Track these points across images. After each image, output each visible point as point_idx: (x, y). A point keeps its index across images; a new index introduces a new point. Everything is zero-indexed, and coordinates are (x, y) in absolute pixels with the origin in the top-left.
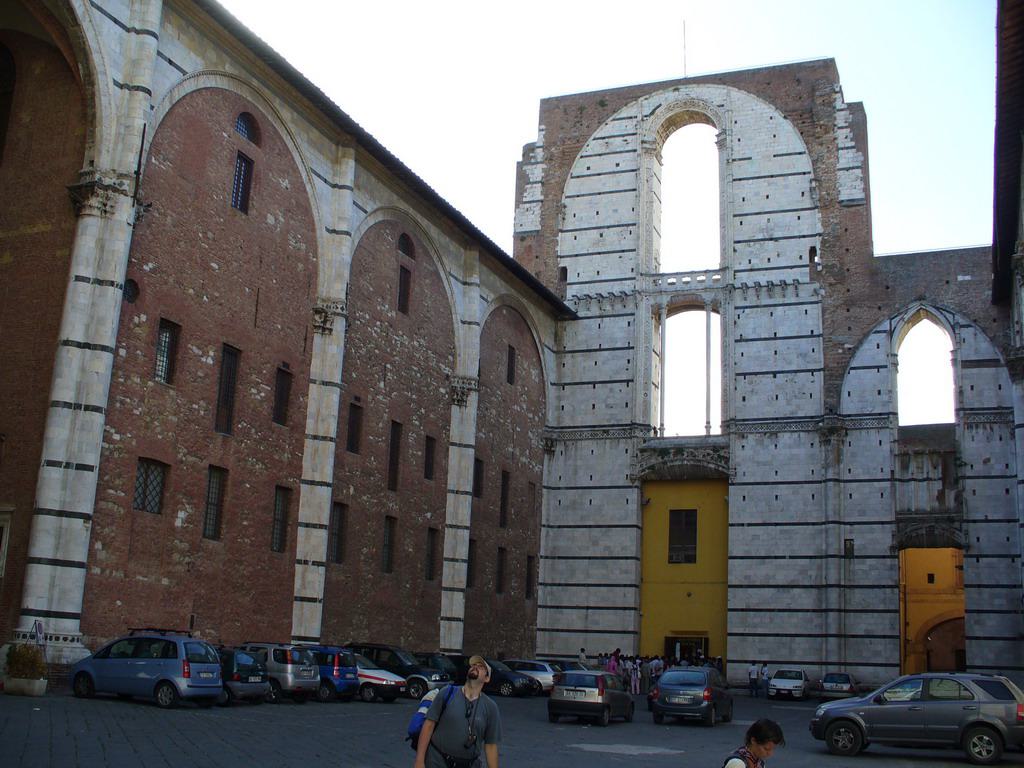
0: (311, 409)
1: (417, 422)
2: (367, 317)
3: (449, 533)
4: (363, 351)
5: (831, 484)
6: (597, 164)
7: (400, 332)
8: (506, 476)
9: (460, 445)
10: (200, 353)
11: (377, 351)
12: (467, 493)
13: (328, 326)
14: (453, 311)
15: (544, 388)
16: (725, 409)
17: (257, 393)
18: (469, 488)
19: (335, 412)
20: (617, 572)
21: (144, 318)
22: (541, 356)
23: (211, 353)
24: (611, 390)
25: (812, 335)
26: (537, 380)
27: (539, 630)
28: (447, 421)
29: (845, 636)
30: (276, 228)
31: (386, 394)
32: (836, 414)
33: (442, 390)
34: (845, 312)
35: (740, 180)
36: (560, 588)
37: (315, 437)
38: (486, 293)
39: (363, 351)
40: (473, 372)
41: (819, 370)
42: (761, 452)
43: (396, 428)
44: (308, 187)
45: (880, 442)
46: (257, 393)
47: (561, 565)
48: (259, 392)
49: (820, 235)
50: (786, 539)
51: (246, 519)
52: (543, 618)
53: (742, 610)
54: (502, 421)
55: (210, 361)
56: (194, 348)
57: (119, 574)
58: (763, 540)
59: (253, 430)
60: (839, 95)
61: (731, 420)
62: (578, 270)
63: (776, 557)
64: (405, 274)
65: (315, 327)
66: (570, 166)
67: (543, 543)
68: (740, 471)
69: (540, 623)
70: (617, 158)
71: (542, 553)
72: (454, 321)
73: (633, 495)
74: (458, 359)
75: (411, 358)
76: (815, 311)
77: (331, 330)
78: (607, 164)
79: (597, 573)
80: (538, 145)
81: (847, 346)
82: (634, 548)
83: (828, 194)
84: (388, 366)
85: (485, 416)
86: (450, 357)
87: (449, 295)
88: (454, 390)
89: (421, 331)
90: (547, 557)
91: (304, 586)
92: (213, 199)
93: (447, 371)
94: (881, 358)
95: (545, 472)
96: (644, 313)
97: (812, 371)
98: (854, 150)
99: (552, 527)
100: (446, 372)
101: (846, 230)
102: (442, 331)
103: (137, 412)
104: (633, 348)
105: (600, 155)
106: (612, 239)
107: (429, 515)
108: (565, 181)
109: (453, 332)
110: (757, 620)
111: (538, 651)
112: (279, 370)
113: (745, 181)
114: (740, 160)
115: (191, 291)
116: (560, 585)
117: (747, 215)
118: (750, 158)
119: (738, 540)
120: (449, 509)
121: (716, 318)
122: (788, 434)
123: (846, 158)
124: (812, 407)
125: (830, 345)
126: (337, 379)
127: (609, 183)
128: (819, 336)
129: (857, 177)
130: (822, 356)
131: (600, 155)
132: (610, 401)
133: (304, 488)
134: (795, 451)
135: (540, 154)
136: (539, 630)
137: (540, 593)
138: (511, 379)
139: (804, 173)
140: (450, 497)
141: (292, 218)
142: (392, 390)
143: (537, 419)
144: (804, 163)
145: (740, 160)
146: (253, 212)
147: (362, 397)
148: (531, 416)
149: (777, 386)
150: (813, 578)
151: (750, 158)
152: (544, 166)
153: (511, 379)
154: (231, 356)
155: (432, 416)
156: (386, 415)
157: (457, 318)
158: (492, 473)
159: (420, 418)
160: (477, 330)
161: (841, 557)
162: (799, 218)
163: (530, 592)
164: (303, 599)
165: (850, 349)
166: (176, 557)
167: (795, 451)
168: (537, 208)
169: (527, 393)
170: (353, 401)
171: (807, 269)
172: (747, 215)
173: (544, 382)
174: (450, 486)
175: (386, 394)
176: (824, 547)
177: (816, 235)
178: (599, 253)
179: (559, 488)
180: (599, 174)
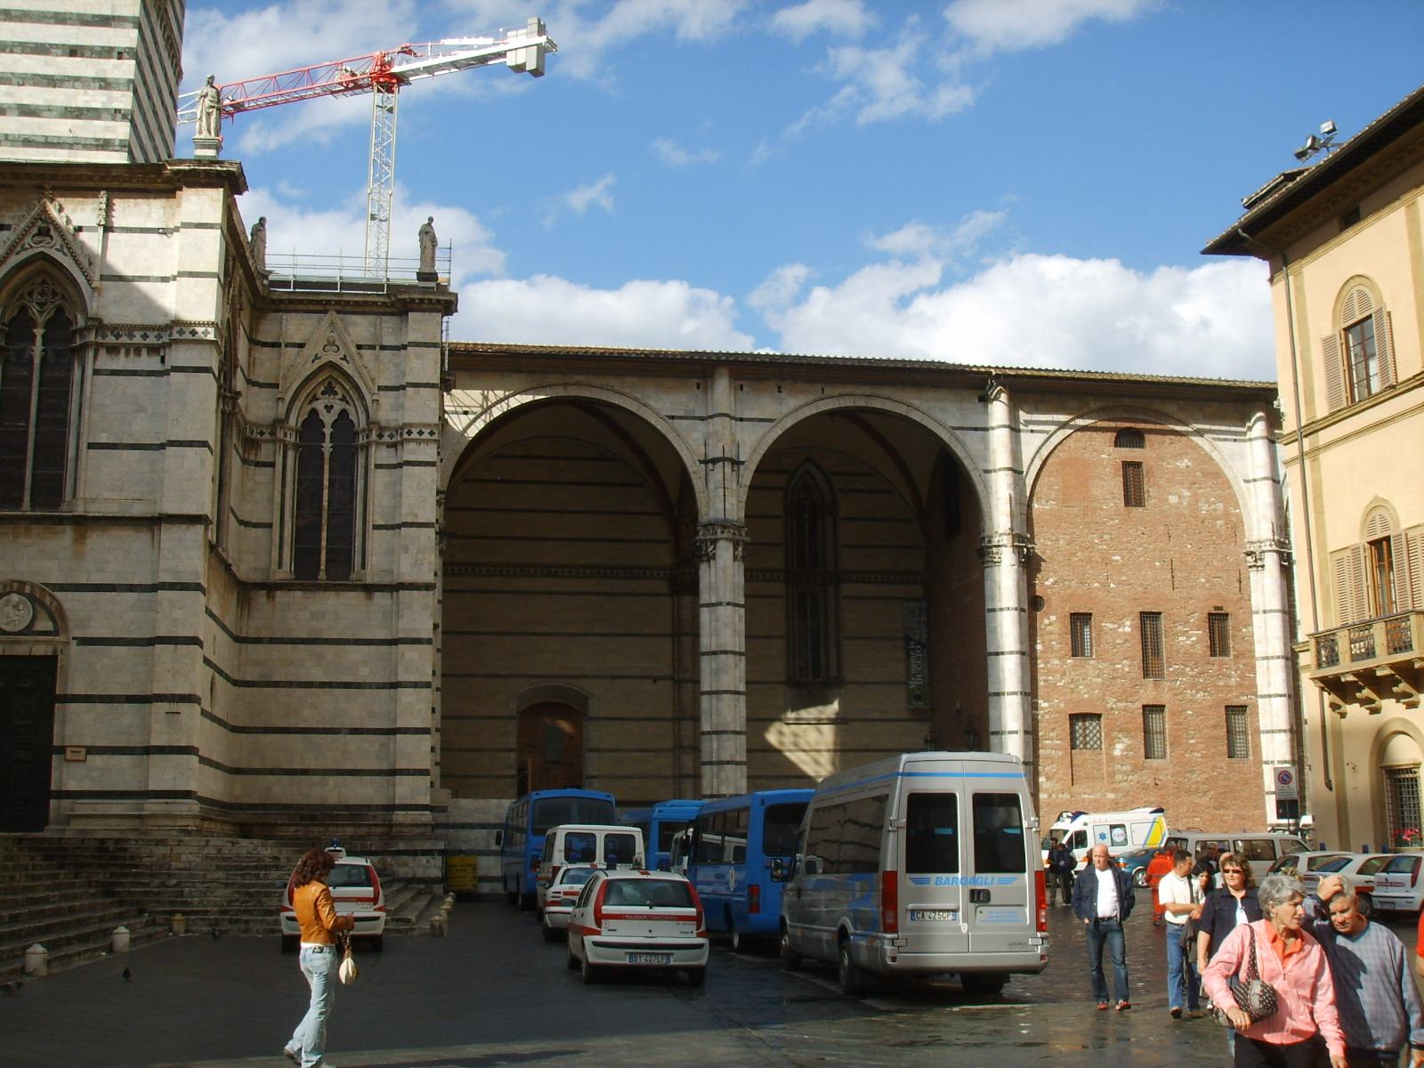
10: (1116, 626)
17: (1187, 637)
23: (1128, 623)
46: (1187, 637)
48: (1189, 637)
51: (1193, 738)
55: (1128, 629)
56: (1108, 625)
57: (1066, 796)
77: (1263, 566)
92: (1102, 509)
112: (1209, 614)
115: (1096, 585)
133: (1260, 701)
154: (1149, 620)
166: (1119, 777)
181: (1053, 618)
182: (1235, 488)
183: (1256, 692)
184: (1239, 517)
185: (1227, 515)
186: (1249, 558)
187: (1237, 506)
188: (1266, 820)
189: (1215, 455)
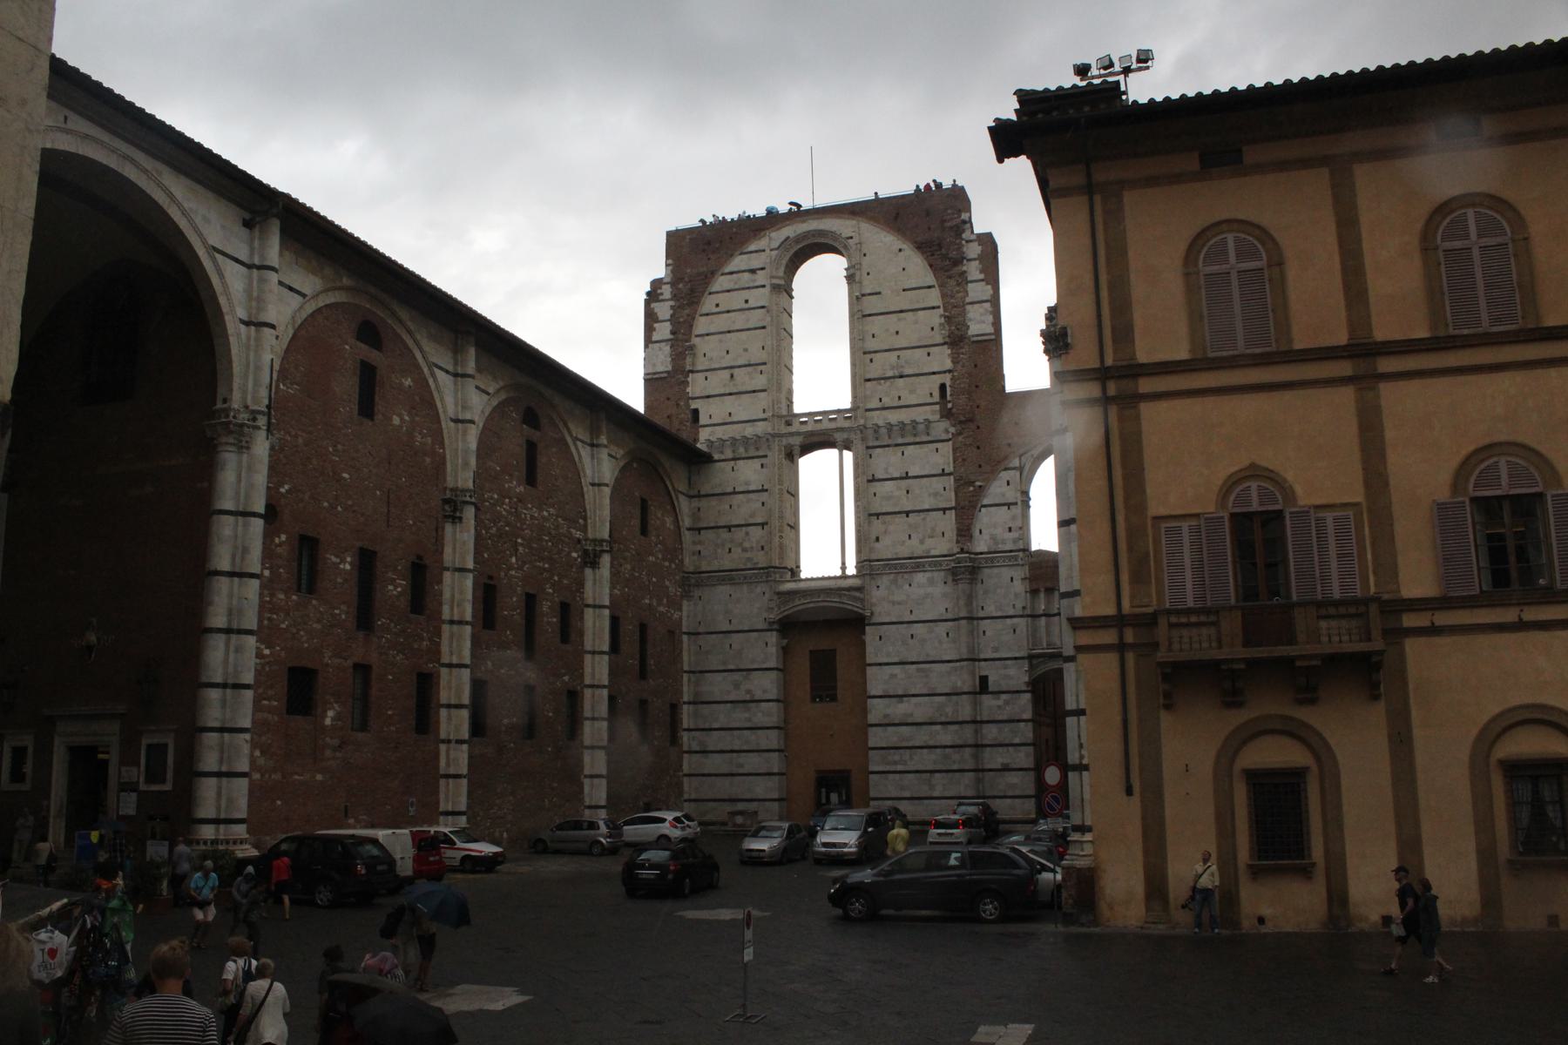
0: (447, 595)
1: (550, 591)
2: (496, 496)
3: (588, 693)
4: (494, 530)
6: (726, 301)
7: (530, 506)
8: (643, 628)
9: (595, 606)
10: (338, 560)
11: (507, 528)
13: (458, 514)
14: (582, 474)
16: (859, 551)
17: (395, 588)
18: (606, 648)
19: (469, 596)
20: (760, 714)
21: (283, 537)
22: (676, 504)
23: (349, 559)
26: (672, 527)
27: (686, 775)
28: (581, 584)
29: (983, 770)
30: (402, 427)
31: (518, 569)
33: (574, 555)
34: (975, 450)
35: (870, 315)
37: (452, 622)
38: (615, 451)
39: (494, 530)
41: (950, 509)
43: (530, 601)
44: (431, 381)
45: (1012, 578)
46: (395, 588)
47: (705, 709)
48: (396, 587)
49: (950, 371)
51: (390, 708)
52: (687, 764)
54: (637, 574)
55: (348, 567)
57: (277, 777)
58: (900, 678)
59: (392, 625)
61: (865, 561)
62: (709, 412)
63: (914, 696)
64: (531, 447)
65: (445, 516)
66: (698, 303)
67: (685, 689)
68: (877, 610)
69: (686, 768)
70: (745, 294)
71: (686, 699)
72: (583, 484)
73: (773, 638)
74: (589, 521)
76: (947, 448)
77: (460, 519)
78: (736, 300)
79: (739, 717)
80: (665, 281)
81: (978, 484)
82: (775, 691)
84: (519, 540)
85: (619, 572)
86: (581, 521)
87: (577, 459)
88: (586, 552)
89: (550, 500)
90: (689, 703)
91: (448, 765)
93: (578, 534)
94: (1011, 495)
95: (685, 619)
96: (775, 455)
97: (944, 510)
98: (983, 283)
99: (693, 672)
100: (578, 536)
101: (976, 366)
103: (283, 626)
104: (766, 490)
105: (728, 291)
106: (745, 379)
107: (566, 678)
108: (694, 318)
110: (897, 758)
111: (686, 796)
112: (413, 563)
114: (870, 294)
115: (326, 504)
116: (703, 730)
117: (876, 352)
118: (879, 293)
119: (877, 681)
120: (588, 670)
121: (848, 456)
123: (977, 291)
124: (943, 545)
125: (962, 483)
126: (470, 565)
127: (739, 320)
128: (950, 474)
129: (986, 310)
130: (953, 494)
131: (728, 291)
132: (747, 545)
133: (444, 671)
135: (666, 291)
136: (686, 775)
137: (685, 739)
138: (644, 531)
139: (934, 308)
140: (588, 658)
141: (417, 415)
142: (524, 563)
143: (673, 566)
144: (934, 298)
145: (870, 294)
146: (379, 417)
148: (667, 564)
149: (910, 526)
150: (950, 714)
151: (879, 293)
152: (672, 303)
153: (644, 531)
154: (367, 561)
155: (565, 582)
158: (629, 628)
159: (553, 586)
160: (607, 491)
161: (975, 693)
162: (929, 354)
163: (674, 739)
164: (447, 776)
166: (328, 753)
168: (667, 349)
171: (937, 407)
172: (876, 352)
174: (588, 647)
175: (518, 569)
177: (945, 372)
178: (730, 394)
179: (699, 634)
180: (728, 312)
181: (283, 537)
183: (439, 659)
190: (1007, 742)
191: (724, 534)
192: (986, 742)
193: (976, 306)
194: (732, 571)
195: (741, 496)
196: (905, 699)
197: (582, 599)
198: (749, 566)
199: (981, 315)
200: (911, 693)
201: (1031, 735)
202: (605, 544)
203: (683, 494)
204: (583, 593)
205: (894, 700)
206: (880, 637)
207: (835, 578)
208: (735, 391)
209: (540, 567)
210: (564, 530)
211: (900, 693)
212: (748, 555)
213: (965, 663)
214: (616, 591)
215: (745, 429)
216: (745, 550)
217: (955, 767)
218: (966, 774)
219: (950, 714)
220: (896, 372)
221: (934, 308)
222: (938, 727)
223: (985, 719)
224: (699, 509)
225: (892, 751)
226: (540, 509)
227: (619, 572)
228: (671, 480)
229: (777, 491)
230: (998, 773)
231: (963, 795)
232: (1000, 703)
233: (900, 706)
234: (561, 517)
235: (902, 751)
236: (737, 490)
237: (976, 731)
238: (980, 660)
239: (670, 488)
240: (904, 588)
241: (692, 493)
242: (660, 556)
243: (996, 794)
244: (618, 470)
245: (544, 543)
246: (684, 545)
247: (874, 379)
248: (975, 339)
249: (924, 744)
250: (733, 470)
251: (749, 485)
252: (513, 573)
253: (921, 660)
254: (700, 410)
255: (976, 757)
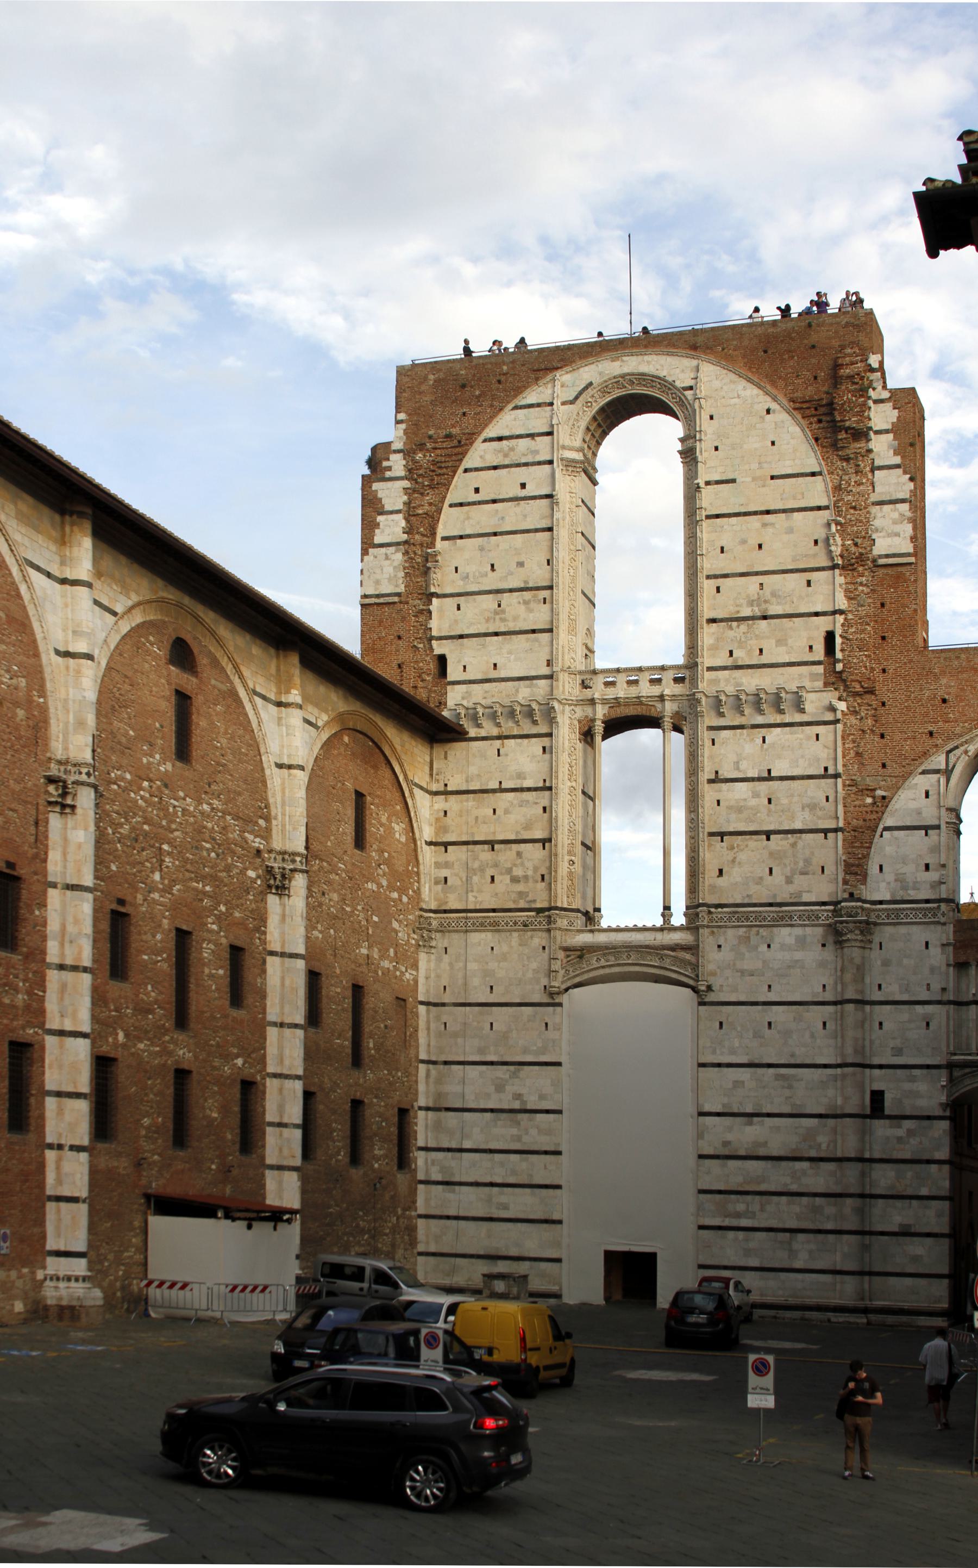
0: (53, 926)
1: (215, 927)
5: (850, 1007)
11: (146, 827)
12: (296, 1026)
14: (262, 750)
15: (415, 850)
19: (88, 928)
24: (519, 854)
25: (825, 775)
26: (403, 839)
28: (261, 919)
31: (163, 890)
32: (859, 900)
33: (251, 874)
34: (877, 739)
36: (450, 1154)
37: (61, 967)
39: (125, 829)
40: (298, 844)
42: (747, 955)
43: (183, 938)
50: (783, 1087)
53: (720, 1192)
60: (879, 374)
63: (769, 1115)
72: (265, 765)
74: (274, 822)
75: (200, 830)
83: (856, 545)
84: (165, 847)
85: (320, 905)
86: (262, 822)
88: (269, 871)
89: (214, 787)
93: (258, 843)
98: (900, 471)
100: (257, 845)
102: (245, 782)
109: (264, 782)
113: (725, 520)
117: (726, 576)
122: (788, 930)
126: (88, 881)
129: (902, 515)
132: (518, 872)
134: (798, 955)
138: (360, 841)
139: (819, 508)
142: (174, 882)
143: (405, 899)
147: (128, 898)
148: (395, 895)
150: (824, 1146)
153: (360, 841)
155: (237, 914)
156: (165, 921)
157: (268, 761)
159: (219, 919)
160: (301, 777)
161: (864, 1116)
162: (809, 583)
165: (884, 798)
167: (798, 955)
169: (387, 862)
170: (114, 906)
172: (726, 576)
173: (415, 841)
175: (163, 890)
176: (839, 1102)
178: (496, 634)
182: (44, 658)
183: (44, 1023)
184: (44, 710)
185: (29, 703)
186: (51, 788)
187: (42, 693)
188: (44, 1245)
189: (23, 589)
190: (909, 1192)
191: (484, 854)
192: (874, 1192)
193: (886, 508)
194: (494, 911)
195: (511, 795)
196: (755, 1119)
197: (264, 942)
198: (522, 904)
199: (895, 523)
200: (764, 1111)
201: (947, 1184)
202: (298, 859)
203: (421, 788)
204: (265, 933)
205: (738, 1119)
206: (721, 1024)
207: (654, 929)
208: (503, 629)
209: (196, 889)
210: (234, 835)
211: (749, 1109)
212: (520, 887)
213: (850, 1070)
214: (316, 933)
215: (517, 691)
216: (515, 880)
217: (830, 1226)
218: (846, 1237)
219: (824, 1146)
220: (756, 609)
221: (819, 508)
222: (805, 1165)
223: (877, 1155)
224: (445, 812)
225: (733, 1196)
226: (199, 802)
227: (320, 905)
228: (401, 766)
229: (567, 791)
230: (894, 1238)
231: (838, 1268)
232: (900, 1132)
233: (748, 1129)
234: (230, 814)
235: (749, 1198)
236: (504, 786)
237: (863, 1174)
238: (872, 1067)
239: (401, 778)
240: (760, 949)
241: (434, 787)
242: (385, 883)
243: (890, 1269)
244: (319, 746)
245: (205, 853)
246: (421, 867)
247: (722, 620)
248: (882, 561)
249: (785, 1190)
250: (499, 755)
251: (525, 778)
252: (156, 896)
253: (782, 1062)
254: (448, 657)
255: (861, 1212)
